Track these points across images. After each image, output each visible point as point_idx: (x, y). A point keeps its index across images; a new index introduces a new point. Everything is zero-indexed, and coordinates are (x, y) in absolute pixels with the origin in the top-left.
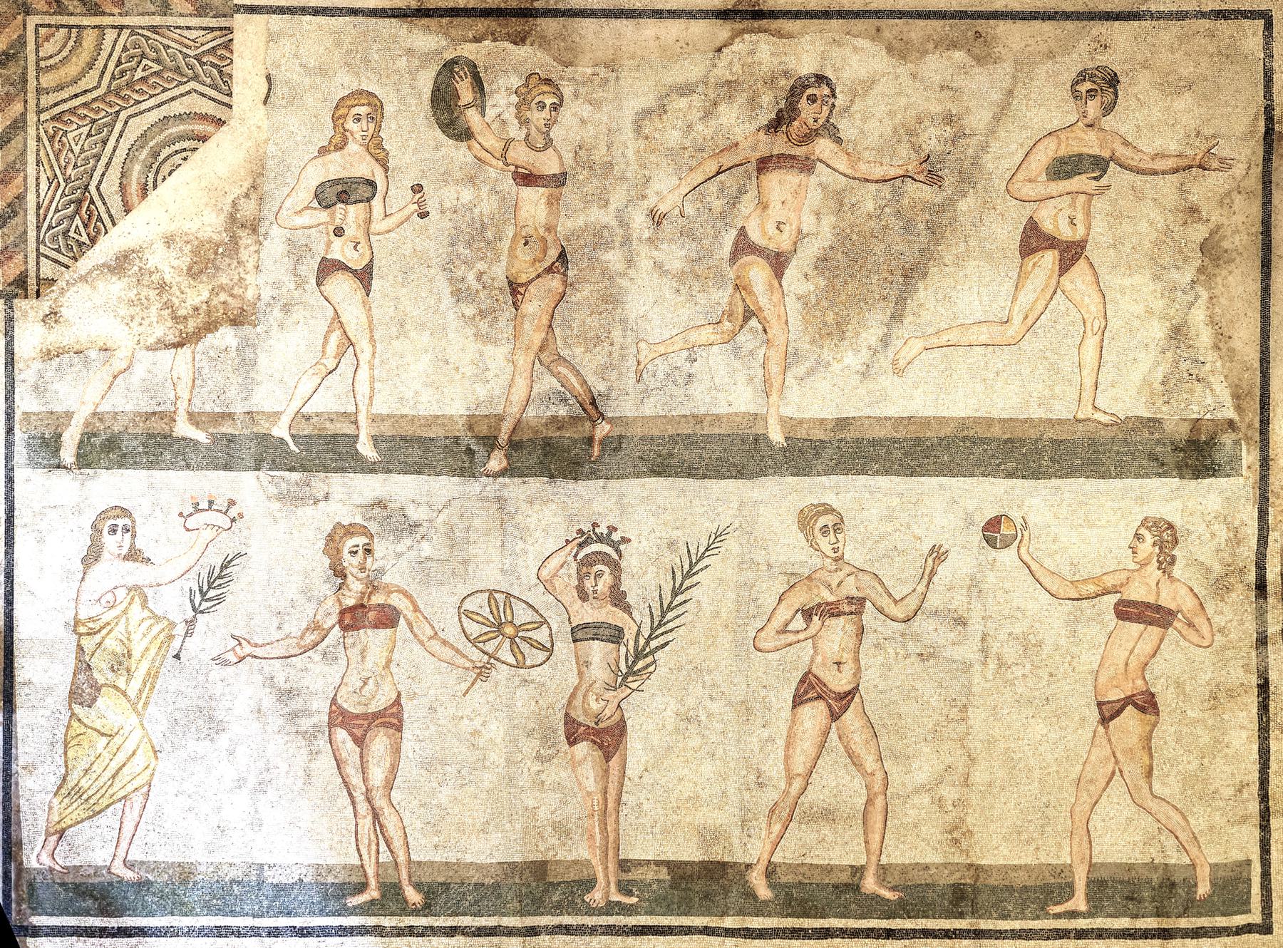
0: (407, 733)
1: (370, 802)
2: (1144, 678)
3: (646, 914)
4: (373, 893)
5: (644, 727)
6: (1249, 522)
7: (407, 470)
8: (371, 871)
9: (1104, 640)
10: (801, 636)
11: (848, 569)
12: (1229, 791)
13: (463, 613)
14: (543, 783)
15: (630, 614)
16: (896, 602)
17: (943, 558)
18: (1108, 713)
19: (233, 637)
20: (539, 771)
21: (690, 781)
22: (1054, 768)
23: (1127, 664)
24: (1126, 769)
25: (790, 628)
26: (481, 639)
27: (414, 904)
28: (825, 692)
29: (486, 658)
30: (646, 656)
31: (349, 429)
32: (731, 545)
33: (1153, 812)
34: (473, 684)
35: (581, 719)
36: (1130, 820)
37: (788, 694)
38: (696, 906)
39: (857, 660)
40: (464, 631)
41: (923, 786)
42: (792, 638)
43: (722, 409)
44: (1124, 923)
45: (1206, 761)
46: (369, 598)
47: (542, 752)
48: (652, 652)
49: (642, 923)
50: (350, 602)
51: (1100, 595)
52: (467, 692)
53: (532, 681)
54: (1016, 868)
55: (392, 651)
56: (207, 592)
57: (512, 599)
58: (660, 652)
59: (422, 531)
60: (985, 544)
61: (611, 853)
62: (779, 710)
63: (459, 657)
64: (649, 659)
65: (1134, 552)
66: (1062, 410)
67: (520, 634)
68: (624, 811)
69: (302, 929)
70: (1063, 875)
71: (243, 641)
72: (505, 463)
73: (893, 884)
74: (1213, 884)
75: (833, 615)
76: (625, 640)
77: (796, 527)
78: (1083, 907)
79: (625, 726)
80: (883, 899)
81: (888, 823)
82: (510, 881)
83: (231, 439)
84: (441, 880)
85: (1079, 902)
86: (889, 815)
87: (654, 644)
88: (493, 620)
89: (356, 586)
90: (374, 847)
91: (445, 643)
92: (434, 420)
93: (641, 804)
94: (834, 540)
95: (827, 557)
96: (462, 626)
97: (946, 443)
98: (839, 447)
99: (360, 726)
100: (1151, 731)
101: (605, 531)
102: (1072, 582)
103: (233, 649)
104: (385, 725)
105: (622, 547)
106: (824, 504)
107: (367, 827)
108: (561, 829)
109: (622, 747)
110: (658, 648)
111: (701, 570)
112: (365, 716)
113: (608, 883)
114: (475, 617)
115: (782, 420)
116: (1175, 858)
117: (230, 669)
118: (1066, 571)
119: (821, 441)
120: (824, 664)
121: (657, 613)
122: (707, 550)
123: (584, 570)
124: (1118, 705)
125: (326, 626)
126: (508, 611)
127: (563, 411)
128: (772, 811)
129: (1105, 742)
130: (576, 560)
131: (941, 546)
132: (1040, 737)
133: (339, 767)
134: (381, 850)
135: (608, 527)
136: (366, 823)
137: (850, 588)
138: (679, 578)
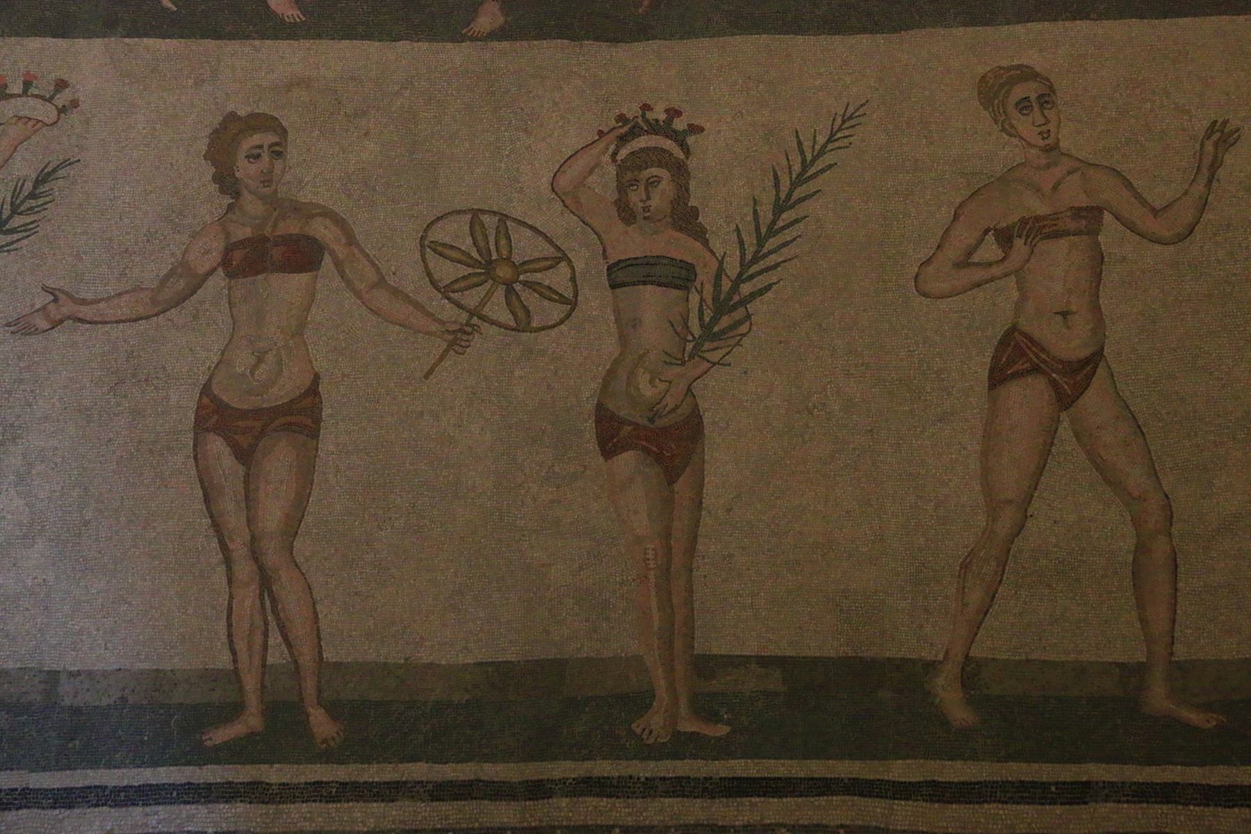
0: (327, 444)
1: (256, 560)
4: (252, 720)
7: (349, 33)
8: (250, 683)
10: (996, 271)
15: (706, 243)
16: (1155, 212)
17: (1231, 140)
19: (45, 289)
20: (552, 502)
25: (976, 258)
26: (456, 287)
27: (325, 741)
28: (1045, 362)
29: (465, 315)
30: (734, 308)
34: (442, 358)
35: (623, 413)
39: (1096, 309)
40: (429, 275)
42: (978, 274)
46: (275, 226)
47: (557, 469)
48: (744, 302)
49: (740, 773)
50: (243, 233)
55: (308, 309)
56: (10, 217)
57: (508, 223)
58: (757, 302)
61: (678, 644)
64: (739, 314)
67: (522, 278)
71: (61, 296)
72: (501, 20)
75: (1049, 237)
81: (1180, 585)
86: (1181, 569)
87: (746, 289)
88: (475, 254)
90: (258, 639)
91: (396, 292)
93: (731, 556)
94: (1042, 121)
95: (1030, 145)
96: (426, 266)
101: (663, 117)
103: (44, 308)
104: (287, 427)
105: (690, 140)
106: (1019, 67)
107: (248, 603)
110: (753, 296)
111: (822, 171)
112: (257, 413)
114: (448, 252)
117: (32, 340)
122: (829, 141)
123: (629, 175)
125: (202, 270)
126: (503, 242)
128: (965, 566)
130: (614, 161)
131: (1225, 123)
133: (207, 499)
134: (271, 642)
135: (667, 111)
136: (248, 599)
137: (1074, 194)
138: (785, 182)
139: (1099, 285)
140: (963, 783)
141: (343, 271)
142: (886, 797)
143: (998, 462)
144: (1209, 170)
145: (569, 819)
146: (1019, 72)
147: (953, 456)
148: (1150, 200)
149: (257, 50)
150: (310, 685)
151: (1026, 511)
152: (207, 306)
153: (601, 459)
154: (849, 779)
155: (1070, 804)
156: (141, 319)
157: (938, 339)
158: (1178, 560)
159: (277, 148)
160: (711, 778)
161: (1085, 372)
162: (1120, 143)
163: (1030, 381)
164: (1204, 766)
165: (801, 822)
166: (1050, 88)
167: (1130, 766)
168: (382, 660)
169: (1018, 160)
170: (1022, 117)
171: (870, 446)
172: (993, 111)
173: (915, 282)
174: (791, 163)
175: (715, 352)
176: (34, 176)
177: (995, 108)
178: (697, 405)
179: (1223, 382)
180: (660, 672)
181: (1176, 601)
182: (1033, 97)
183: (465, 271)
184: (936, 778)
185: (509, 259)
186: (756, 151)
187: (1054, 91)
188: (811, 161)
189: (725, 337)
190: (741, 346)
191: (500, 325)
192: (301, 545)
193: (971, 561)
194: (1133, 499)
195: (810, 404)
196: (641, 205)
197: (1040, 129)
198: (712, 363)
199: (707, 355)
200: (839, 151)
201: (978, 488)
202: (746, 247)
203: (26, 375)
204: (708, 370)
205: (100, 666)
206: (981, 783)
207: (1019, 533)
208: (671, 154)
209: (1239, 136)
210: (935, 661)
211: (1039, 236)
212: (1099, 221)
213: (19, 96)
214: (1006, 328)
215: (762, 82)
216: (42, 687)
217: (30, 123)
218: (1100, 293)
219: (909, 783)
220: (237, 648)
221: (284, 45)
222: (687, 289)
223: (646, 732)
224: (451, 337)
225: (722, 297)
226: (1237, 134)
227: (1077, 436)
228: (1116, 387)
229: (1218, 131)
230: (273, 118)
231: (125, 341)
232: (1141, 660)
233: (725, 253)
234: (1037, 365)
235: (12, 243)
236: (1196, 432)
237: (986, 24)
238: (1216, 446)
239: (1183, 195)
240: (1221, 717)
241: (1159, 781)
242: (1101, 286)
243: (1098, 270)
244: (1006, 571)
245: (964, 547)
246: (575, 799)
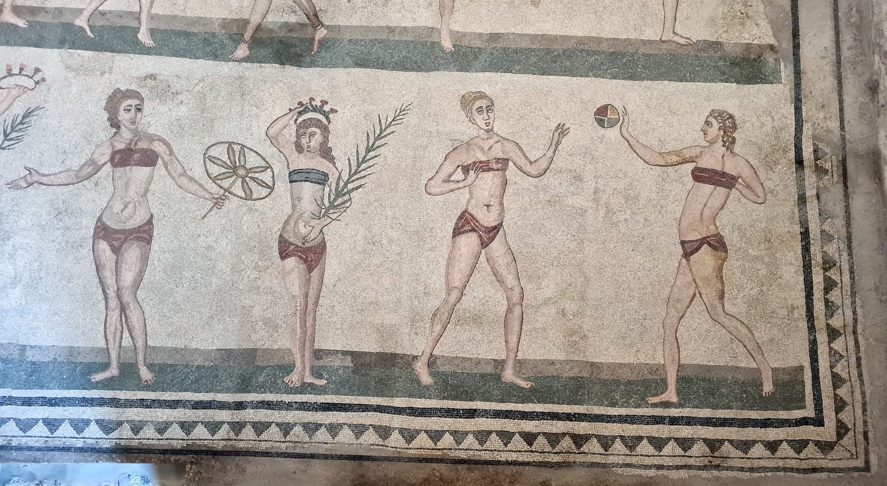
0: (155, 245)
2: (715, 225)
3: (332, 394)
4: (113, 371)
5: (340, 247)
6: (789, 116)
7: (176, 54)
8: (114, 355)
9: (684, 196)
10: (461, 185)
11: (496, 138)
12: (784, 312)
13: (208, 158)
14: (258, 288)
16: (531, 163)
17: (565, 133)
18: (689, 250)
20: (256, 278)
21: (372, 289)
22: (650, 289)
23: (702, 214)
24: (703, 292)
26: (219, 177)
27: (146, 381)
28: (477, 226)
29: (222, 191)
30: (344, 194)
31: (134, 24)
32: (411, 119)
33: (726, 326)
34: (210, 210)
35: (291, 240)
36: (709, 331)
37: (450, 226)
38: (373, 388)
40: (207, 171)
41: (550, 299)
42: (453, 186)
43: (408, 24)
44: (705, 413)
45: (764, 288)
46: (136, 144)
47: (259, 263)
48: (349, 192)
50: (120, 146)
51: (680, 164)
52: (205, 216)
53: (256, 210)
54: (621, 366)
55: (150, 184)
57: (245, 149)
59: (180, 97)
60: (596, 124)
61: (307, 344)
62: (442, 238)
63: (201, 189)
64: (346, 197)
65: (705, 134)
66: (651, 33)
67: (250, 175)
68: (320, 311)
69: (50, 400)
70: (658, 373)
72: (248, 53)
74: (775, 384)
75: (484, 171)
76: (329, 183)
78: (674, 399)
79: (325, 246)
80: (518, 387)
81: (523, 327)
82: (226, 364)
83: (43, 25)
84: (169, 362)
85: (671, 395)
87: (350, 186)
88: (229, 163)
89: (126, 134)
90: (118, 334)
91: (191, 179)
92: (198, 21)
95: (481, 129)
96: (206, 167)
97: (569, 54)
98: (492, 53)
99: (119, 239)
100: (722, 265)
101: (319, 104)
102: (660, 154)
103: (25, 177)
104: (138, 239)
105: (331, 116)
106: (479, 92)
107: (114, 318)
108: (271, 324)
109: (322, 261)
110: (353, 189)
111: (389, 134)
112: (123, 232)
113: (304, 368)
114: (216, 161)
115: (451, 31)
116: (745, 363)
117: (19, 192)
118: (655, 144)
119: (479, 49)
120: (477, 206)
121: (354, 164)
122: (393, 120)
123: (302, 131)
124: (696, 244)
125: (100, 163)
126: (242, 158)
127: (293, 19)
128: (435, 315)
129: (687, 271)
130: (296, 123)
131: (564, 125)
132: (638, 265)
133: (97, 269)
134: (124, 336)
135: (321, 101)
136: (115, 315)
137: (498, 152)
141: (167, 167)
145: (253, 419)
148: (529, 157)
149: (131, 59)
150: (141, 357)
152: (102, 180)
153: (280, 260)
155: (467, 418)
156: (70, 184)
157: (432, 214)
159: (138, 107)
165: (354, 423)
168: (175, 346)
169: (475, 135)
176: (22, 114)
178: (324, 238)
180: (298, 356)
182: (484, 107)
183: (225, 170)
185: (244, 166)
191: (238, 196)
192: (141, 294)
196: (306, 145)
197: (486, 122)
199: (330, 215)
201: (443, 281)
203: (15, 209)
205: (45, 344)
208: (322, 122)
213: (17, 75)
216: (19, 351)
217: (22, 88)
220: (108, 338)
221: (145, 57)
222: (324, 185)
223: (290, 382)
224: (216, 201)
225: (340, 189)
230: (137, 92)
231: (62, 194)
235: (12, 145)
237: (467, 71)
246: (256, 410)
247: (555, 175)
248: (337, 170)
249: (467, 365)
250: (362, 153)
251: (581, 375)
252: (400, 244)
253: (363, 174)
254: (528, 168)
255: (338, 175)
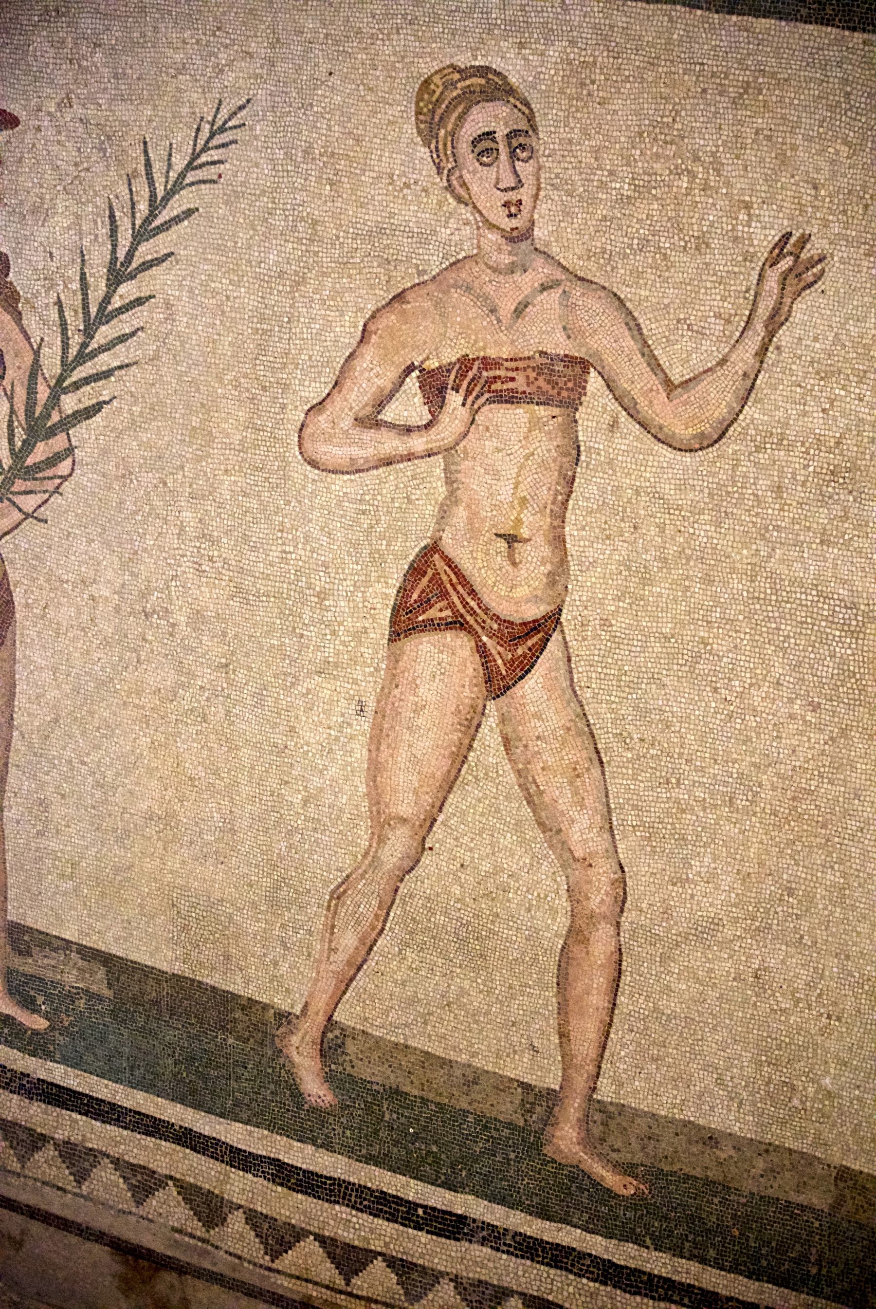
10: (418, 443)
11: (541, 271)
15: (18, 316)
16: (669, 385)
17: (809, 276)
25: (388, 415)
28: (474, 613)
30: (52, 433)
39: (558, 541)
41: (716, 923)
42: (391, 444)
64: (58, 442)
73: (625, 1157)
77: (410, 129)
80: (596, 1185)
81: (621, 999)
86: (626, 979)
87: (70, 403)
94: (509, 181)
95: (492, 226)
111: (177, 220)
120: (473, 531)
121: (76, 322)
122: (190, 167)
128: (338, 896)
139: (567, 501)
140: (312, 1173)
142: (223, 1161)
143: (392, 756)
144: (766, 327)
146: (483, 81)
147: (332, 732)
151: (424, 839)
154: (181, 1127)
158: (624, 963)
160: (28, 1075)
161: (530, 643)
162: (630, 246)
163: (449, 639)
164: (611, 1238)
166: (529, 121)
167: (518, 1212)
169: (468, 249)
170: (480, 168)
171: (223, 690)
172: (437, 148)
173: (299, 437)
174: (135, 199)
175: (29, 496)
177: (441, 147)
179: (732, 708)
181: (612, 1021)
182: (501, 133)
184: (281, 1157)
186: (88, 170)
187: (535, 129)
188: (163, 198)
189: (40, 475)
190: (61, 494)
193: (345, 891)
194: (576, 860)
195: (149, 606)
198: (24, 513)
199: (15, 499)
200: (203, 186)
201: (363, 789)
202: (70, 333)
204: (20, 524)
206: (335, 1179)
207: (412, 869)
209: (823, 271)
210: (290, 1014)
211: (487, 396)
212: (580, 387)
214: (422, 545)
215: (100, 46)
218: (567, 515)
219: (250, 1153)
226: (819, 267)
227: (507, 742)
228: (572, 680)
229: (791, 254)
232: (553, 1086)
233: (42, 339)
234: (462, 616)
236: (678, 780)
238: (704, 810)
239: (718, 364)
240: (642, 1187)
241: (551, 1240)
242: (571, 502)
243: (570, 473)
244: (391, 918)
245: (337, 870)
247: (758, 449)
248: (28, 338)
249: (439, 1076)
250: (98, 288)
251: (801, 1199)
252: (224, 634)
253: (104, 361)
254: (657, 408)
255: (29, 359)
